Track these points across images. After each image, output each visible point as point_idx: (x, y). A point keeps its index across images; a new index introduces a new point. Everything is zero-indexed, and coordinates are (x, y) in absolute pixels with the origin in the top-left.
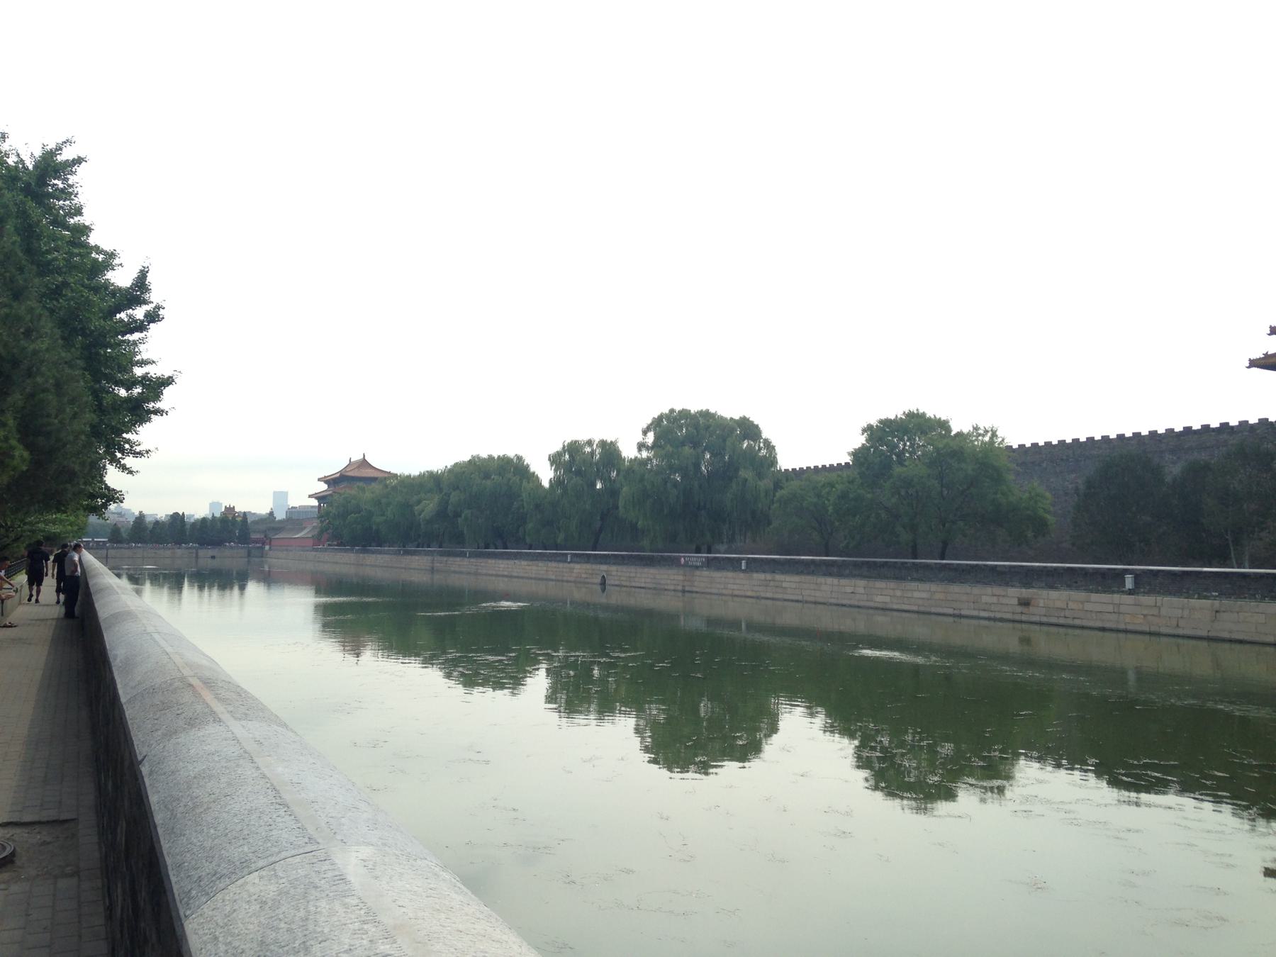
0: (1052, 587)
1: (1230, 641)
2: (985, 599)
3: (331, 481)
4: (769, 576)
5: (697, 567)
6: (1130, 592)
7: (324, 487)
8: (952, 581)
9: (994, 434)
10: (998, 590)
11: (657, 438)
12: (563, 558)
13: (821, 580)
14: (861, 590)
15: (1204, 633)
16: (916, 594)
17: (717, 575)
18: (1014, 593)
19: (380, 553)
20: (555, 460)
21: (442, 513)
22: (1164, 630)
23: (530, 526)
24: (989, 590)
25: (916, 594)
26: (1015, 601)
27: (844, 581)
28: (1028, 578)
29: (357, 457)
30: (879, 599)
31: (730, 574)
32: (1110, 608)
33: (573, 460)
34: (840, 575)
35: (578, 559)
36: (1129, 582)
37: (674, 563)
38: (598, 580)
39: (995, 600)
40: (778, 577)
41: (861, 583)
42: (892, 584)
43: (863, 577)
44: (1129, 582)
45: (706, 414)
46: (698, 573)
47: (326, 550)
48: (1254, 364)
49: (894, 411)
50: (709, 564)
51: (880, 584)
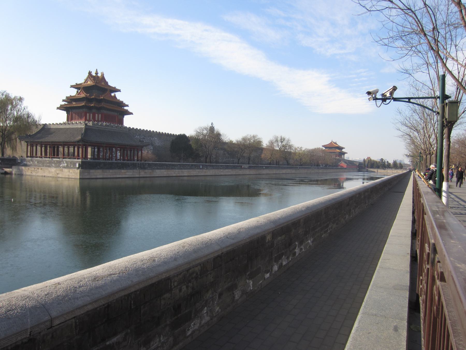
48: (58, 108)
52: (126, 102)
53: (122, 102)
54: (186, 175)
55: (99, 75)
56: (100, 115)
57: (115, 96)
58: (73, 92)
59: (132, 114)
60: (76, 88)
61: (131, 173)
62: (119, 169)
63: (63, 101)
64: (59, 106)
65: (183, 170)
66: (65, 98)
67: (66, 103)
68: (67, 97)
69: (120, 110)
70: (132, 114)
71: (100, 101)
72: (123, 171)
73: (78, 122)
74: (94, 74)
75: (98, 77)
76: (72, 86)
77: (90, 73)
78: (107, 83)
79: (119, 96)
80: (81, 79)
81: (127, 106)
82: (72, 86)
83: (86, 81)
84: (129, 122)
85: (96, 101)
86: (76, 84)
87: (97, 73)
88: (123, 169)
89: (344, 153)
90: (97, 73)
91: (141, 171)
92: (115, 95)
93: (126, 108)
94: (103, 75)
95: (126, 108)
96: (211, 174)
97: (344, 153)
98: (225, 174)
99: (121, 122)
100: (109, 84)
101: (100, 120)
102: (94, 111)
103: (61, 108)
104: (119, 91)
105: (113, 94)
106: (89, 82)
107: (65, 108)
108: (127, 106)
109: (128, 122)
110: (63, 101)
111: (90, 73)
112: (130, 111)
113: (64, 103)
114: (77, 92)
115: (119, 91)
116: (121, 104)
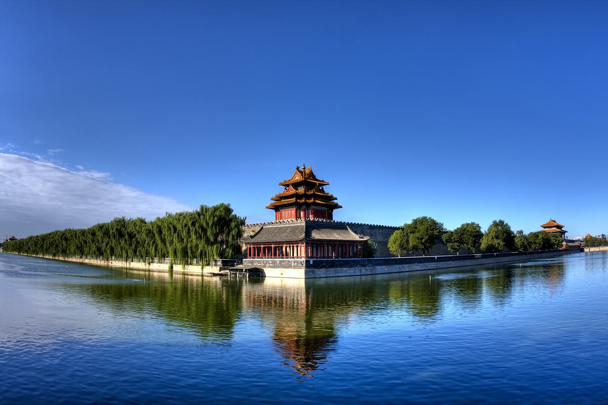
52: (335, 196)
54: (407, 270)
57: (322, 191)
58: (281, 191)
59: (341, 207)
60: (284, 185)
61: (353, 271)
62: (340, 267)
63: (272, 199)
64: (268, 205)
65: (404, 265)
70: (341, 207)
71: (307, 197)
72: (344, 269)
77: (298, 168)
78: (314, 178)
79: (328, 190)
81: (336, 199)
87: (304, 168)
88: (345, 267)
89: (564, 232)
90: (304, 168)
91: (362, 268)
92: (323, 188)
93: (335, 201)
95: (335, 201)
96: (433, 268)
97: (564, 232)
98: (447, 266)
99: (330, 217)
100: (317, 178)
102: (304, 207)
104: (328, 184)
106: (297, 178)
107: (275, 206)
108: (336, 199)
109: (338, 216)
110: (272, 199)
111: (298, 168)
112: (339, 204)
113: (273, 202)
114: (285, 188)
116: (331, 198)
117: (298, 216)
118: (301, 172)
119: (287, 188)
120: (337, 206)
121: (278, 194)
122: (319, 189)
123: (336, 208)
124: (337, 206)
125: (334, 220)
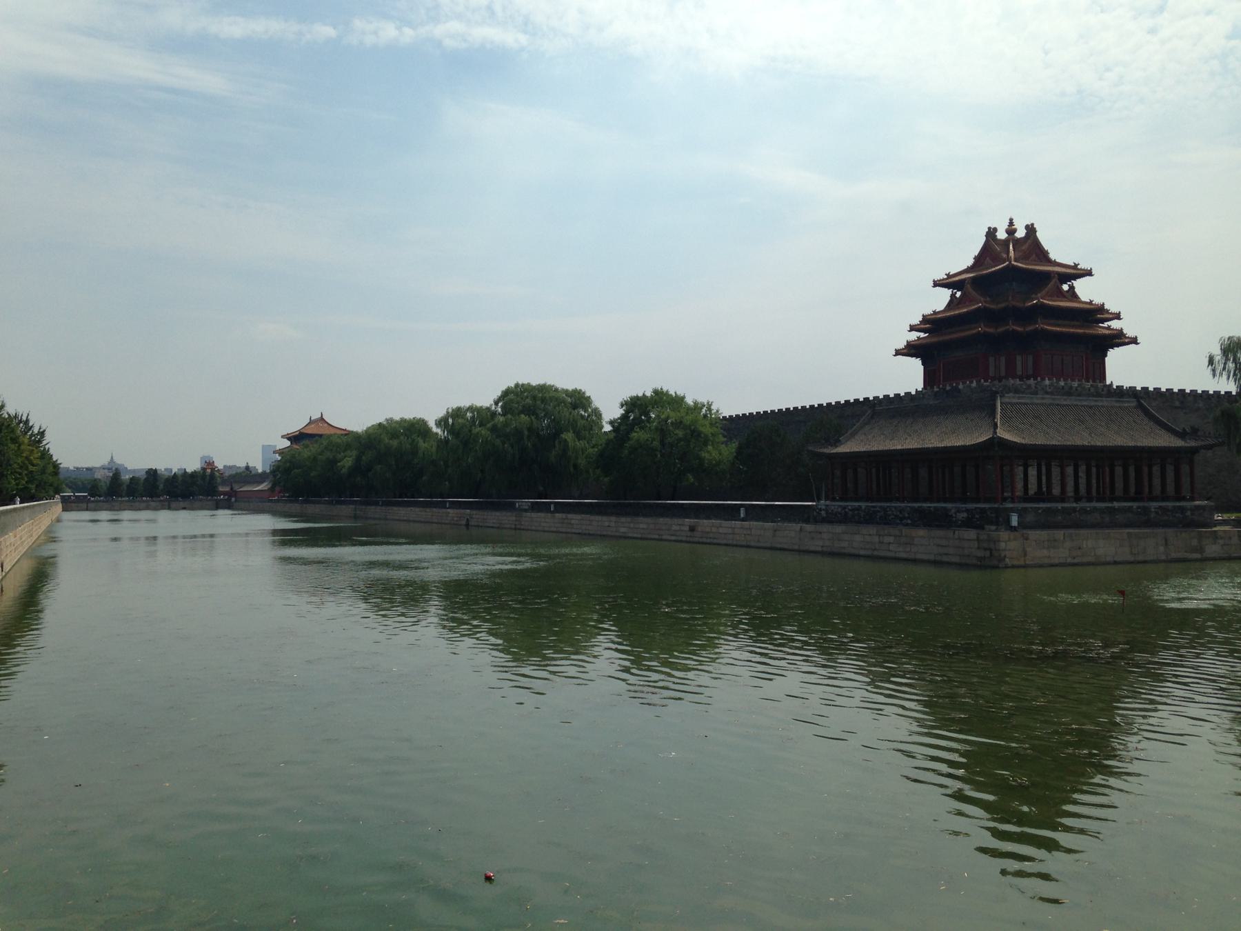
0: (708, 518)
1: (781, 549)
2: (675, 528)
3: (296, 438)
4: (564, 516)
5: (526, 511)
6: (743, 520)
7: (288, 443)
8: (662, 515)
9: (709, 409)
10: (680, 521)
11: (502, 407)
12: (442, 505)
13: (592, 518)
14: (613, 524)
15: (768, 545)
16: (642, 526)
17: (534, 515)
18: (688, 521)
19: (319, 503)
20: (441, 422)
21: (357, 469)
22: (753, 544)
23: (424, 478)
24: (676, 521)
25: (642, 526)
26: (687, 528)
27: (605, 518)
28: (699, 511)
29: (316, 416)
30: (623, 530)
31: (542, 515)
32: (730, 531)
33: (456, 420)
34: (591, 513)
35: (454, 505)
36: (742, 511)
37: (511, 507)
38: (464, 522)
39: (677, 528)
40: (570, 516)
41: (613, 519)
42: (629, 519)
43: (612, 514)
44: (742, 511)
45: (543, 388)
46: (524, 514)
47: (278, 501)
48: (898, 353)
49: (645, 389)
50: (536, 508)
51: (623, 519)
52: (1111, 307)
53: (1101, 309)
55: (1021, 233)
56: (1030, 358)
58: (940, 300)
59: (1134, 341)
66: (916, 320)
67: (922, 335)
68: (926, 319)
69: (1093, 334)
70: (1134, 341)
73: (961, 386)
74: (1002, 235)
75: (1017, 242)
76: (937, 284)
77: (991, 233)
78: (1042, 255)
79: (1085, 290)
80: (962, 258)
81: (1117, 316)
82: (937, 284)
83: (979, 260)
84: (1121, 368)
85: (1013, 315)
86: (949, 276)
87: (1011, 231)
90: (1011, 231)
92: (1072, 288)
93: (1115, 324)
94: (1031, 229)
95: (1115, 324)
100: (1052, 256)
101: (1030, 372)
103: (911, 350)
104: (1089, 273)
105: (1065, 287)
108: (1117, 316)
109: (1121, 368)
112: (1129, 332)
113: (914, 336)
114: (953, 296)
115: (1089, 273)
116: (1096, 313)
117: (991, 374)
118: (1005, 243)
119: (958, 294)
120: (1118, 339)
121: (928, 311)
122: (1061, 290)
123: (1119, 345)
124: (1118, 339)
125: (1108, 382)
